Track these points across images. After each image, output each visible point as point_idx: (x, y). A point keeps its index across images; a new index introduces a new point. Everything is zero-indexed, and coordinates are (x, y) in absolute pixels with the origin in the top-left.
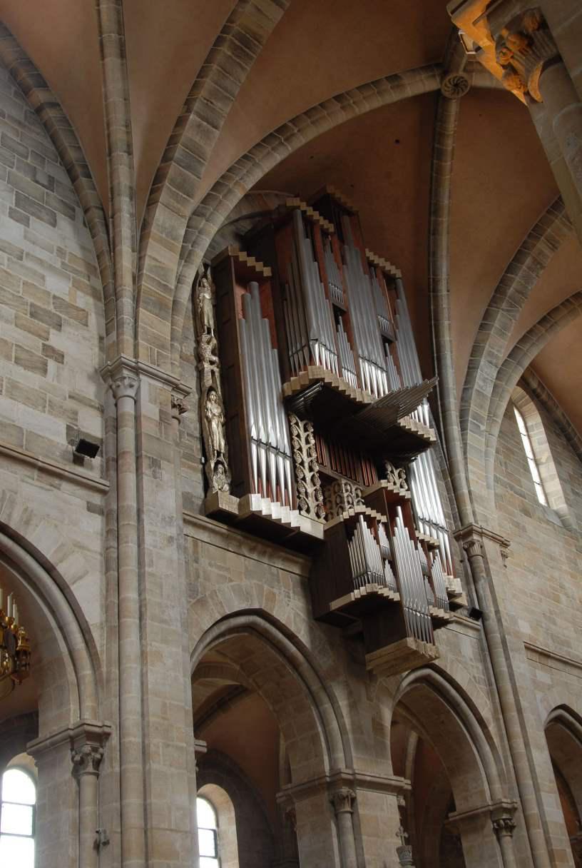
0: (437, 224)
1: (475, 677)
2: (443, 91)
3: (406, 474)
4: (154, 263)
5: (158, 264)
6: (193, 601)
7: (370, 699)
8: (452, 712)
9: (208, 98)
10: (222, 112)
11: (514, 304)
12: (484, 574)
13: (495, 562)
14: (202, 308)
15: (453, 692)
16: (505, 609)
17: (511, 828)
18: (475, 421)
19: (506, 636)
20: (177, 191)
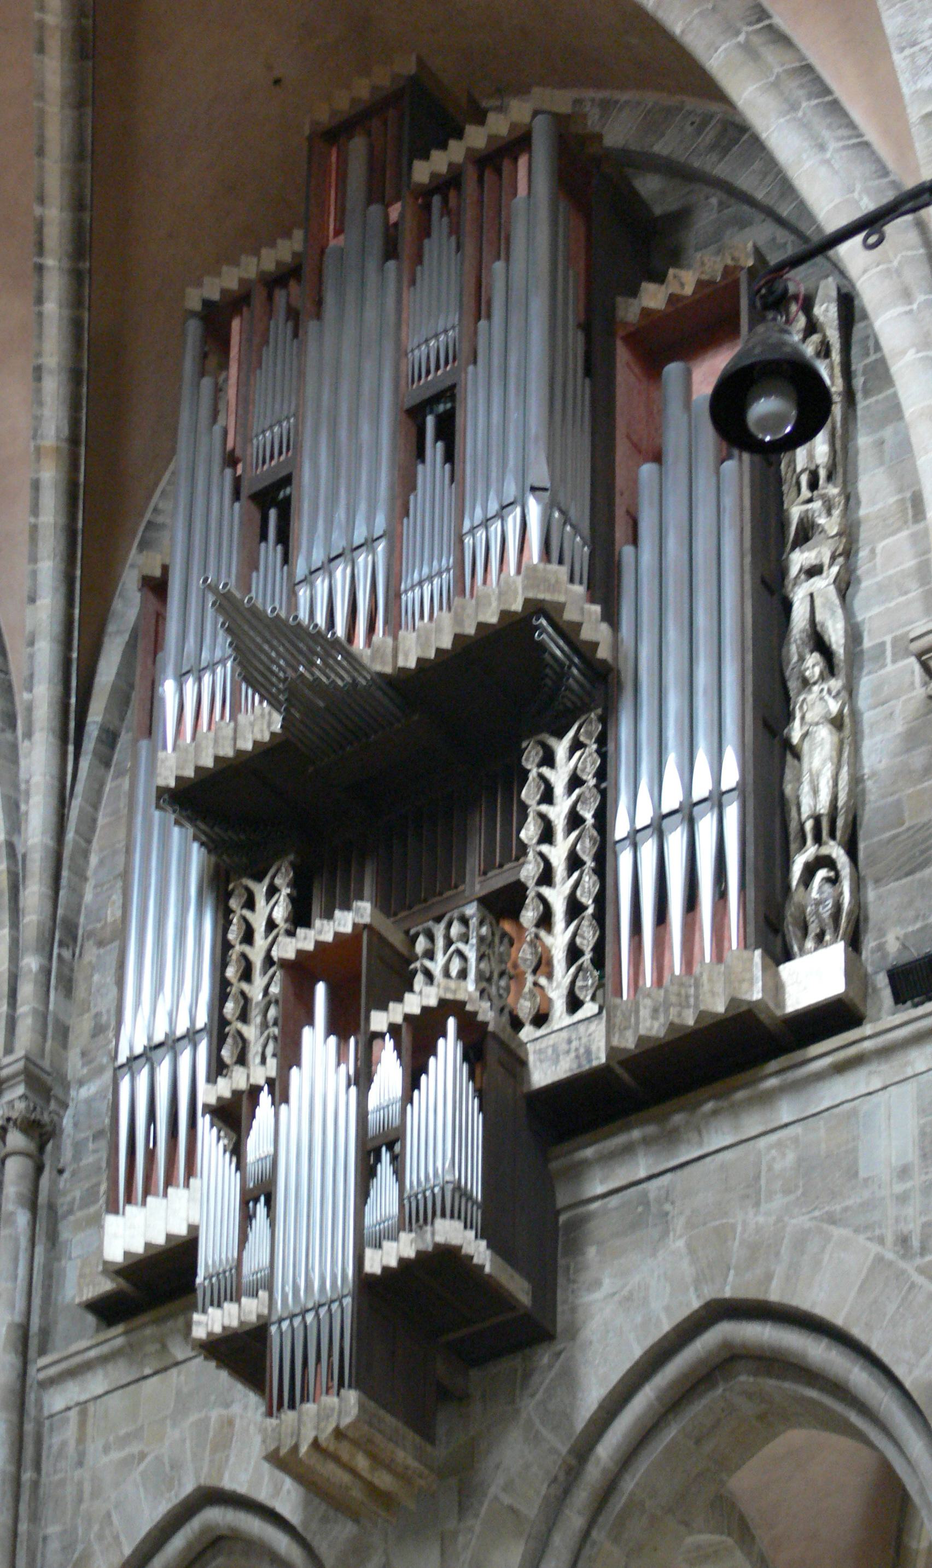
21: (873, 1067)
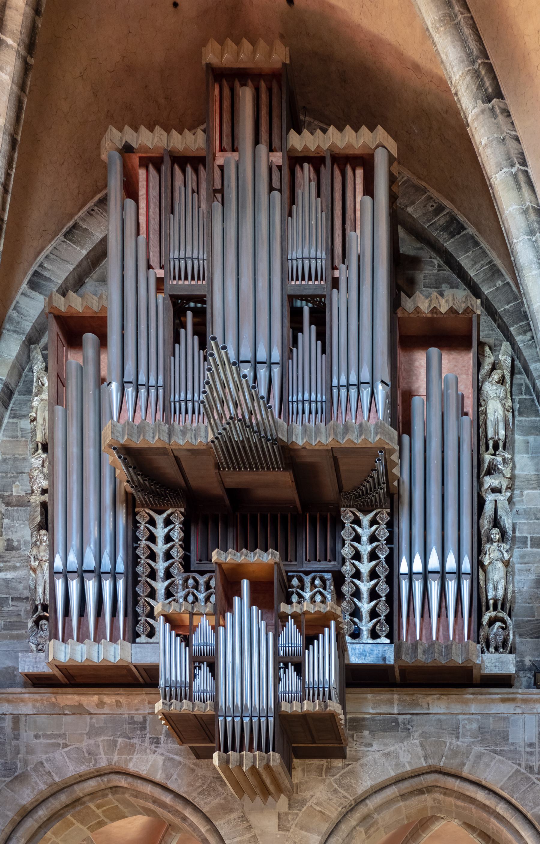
6: (8, 780)
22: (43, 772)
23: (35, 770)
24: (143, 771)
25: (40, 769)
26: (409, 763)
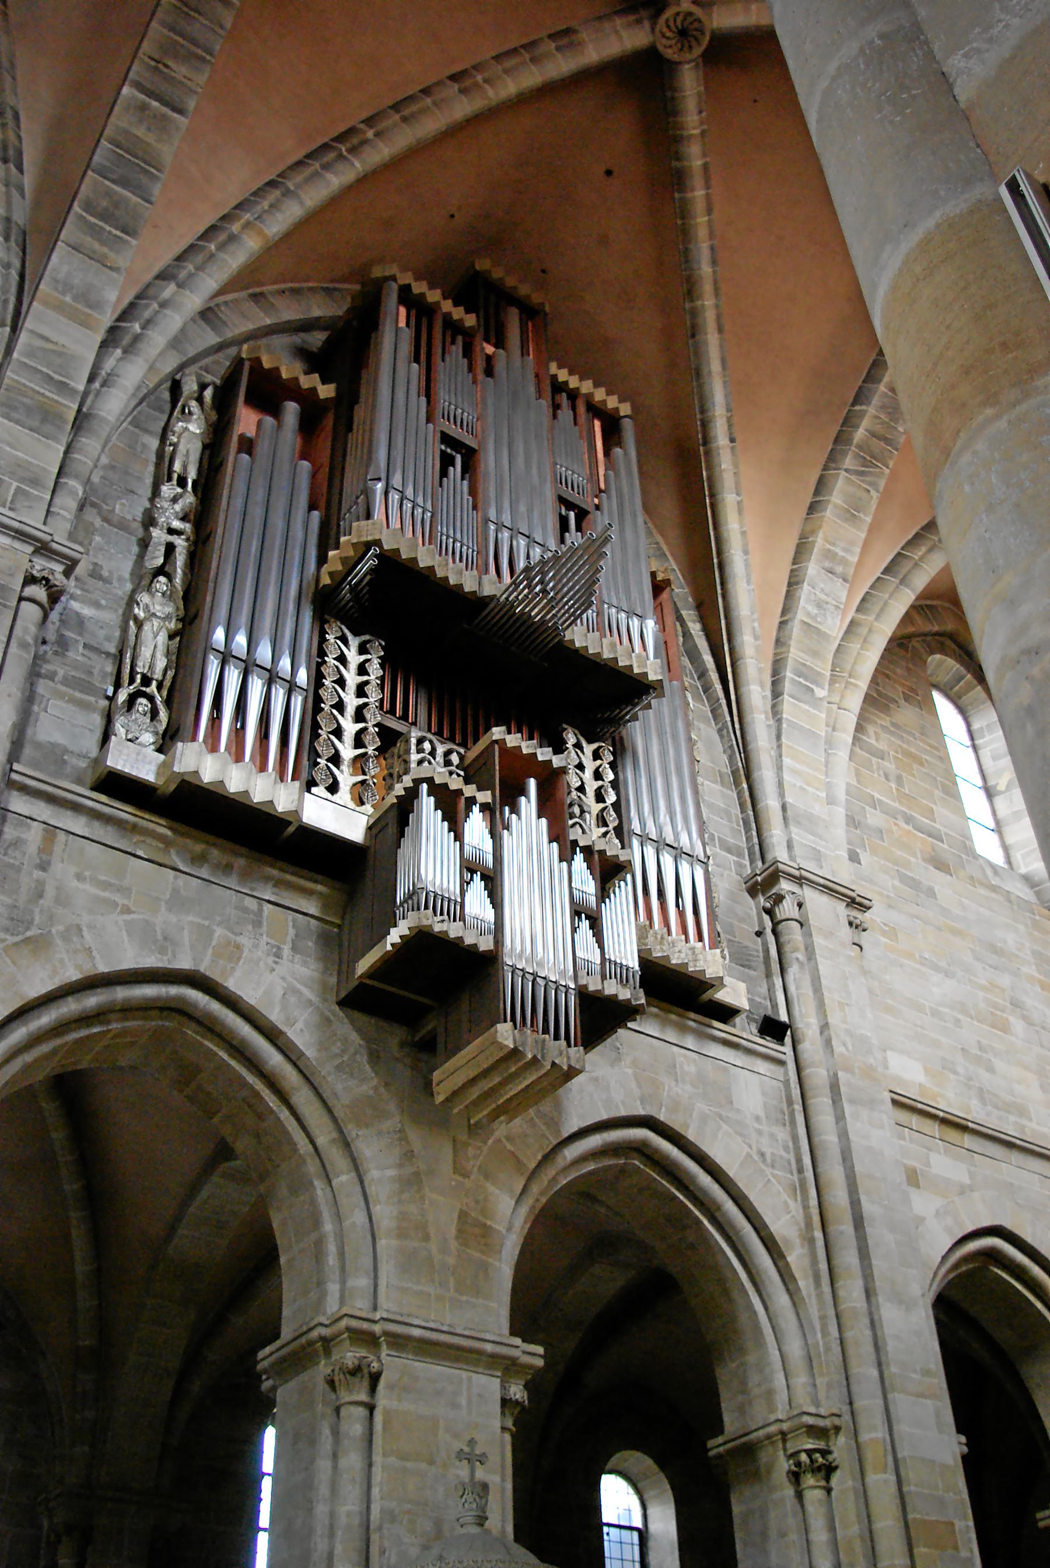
0: (694, 313)
1: (762, 1155)
2: (661, 48)
3: (614, 754)
4: (39, 343)
5: (50, 346)
6: (11, 939)
7: (458, 1169)
8: (706, 1222)
9: (156, 57)
10: (189, 83)
11: (869, 460)
12: (801, 956)
13: (829, 934)
14: (175, 445)
15: (705, 1180)
16: (844, 1022)
17: (829, 1470)
18: (801, 680)
19: (840, 1074)
20: (101, 223)
21: (739, 1053)
22: (78, 946)
23: (66, 937)
24: (250, 995)
25: (75, 939)
26: (623, 1103)
